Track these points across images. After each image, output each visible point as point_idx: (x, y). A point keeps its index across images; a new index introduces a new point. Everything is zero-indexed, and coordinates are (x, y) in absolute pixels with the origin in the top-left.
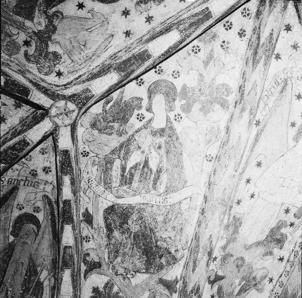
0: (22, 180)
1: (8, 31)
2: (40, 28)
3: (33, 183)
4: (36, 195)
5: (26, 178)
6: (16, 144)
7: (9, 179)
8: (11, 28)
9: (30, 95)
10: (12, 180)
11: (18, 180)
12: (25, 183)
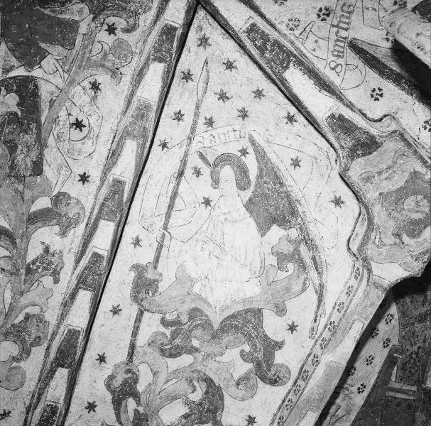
0: (338, 32)
1: (100, 56)
2: (86, 11)
3: (345, 14)
4: (368, 9)
5: (333, 26)
6: (255, 45)
7: (334, 56)
8: (94, 53)
9: (173, 24)
10: (335, 50)
11: (336, 41)
12: (342, 28)
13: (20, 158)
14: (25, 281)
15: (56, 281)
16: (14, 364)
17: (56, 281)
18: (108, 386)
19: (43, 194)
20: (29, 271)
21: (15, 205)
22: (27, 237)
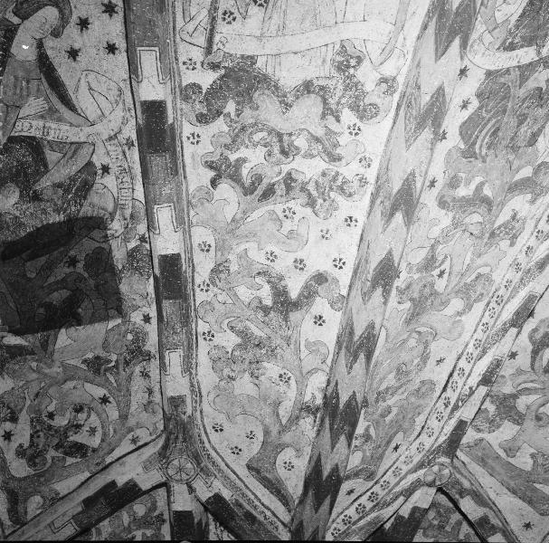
13: (522, 130)
14: (486, 244)
15: (512, 245)
16: (458, 318)
17: (512, 245)
18: (531, 338)
19: (528, 163)
20: (493, 235)
21: (502, 175)
22: (503, 204)
